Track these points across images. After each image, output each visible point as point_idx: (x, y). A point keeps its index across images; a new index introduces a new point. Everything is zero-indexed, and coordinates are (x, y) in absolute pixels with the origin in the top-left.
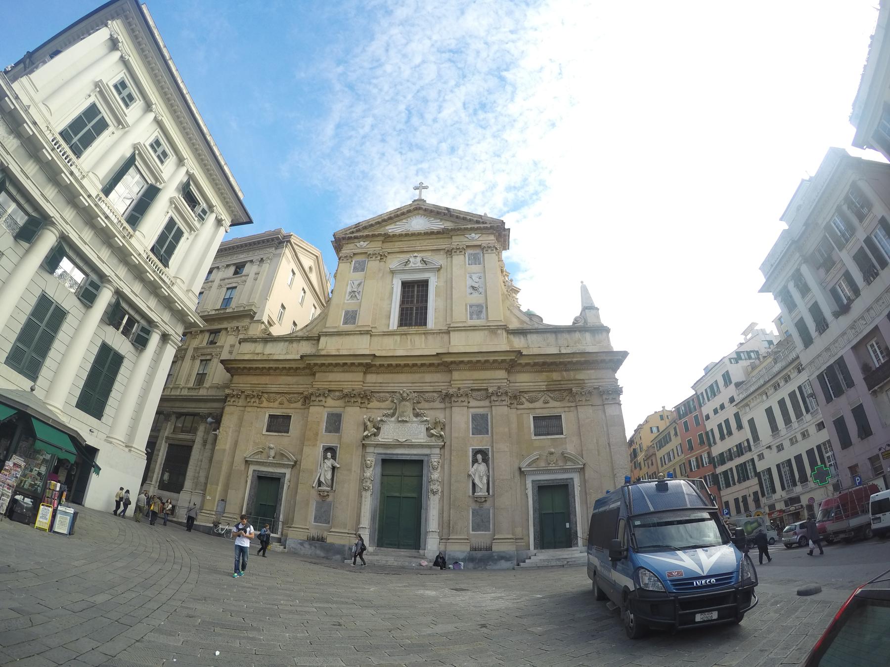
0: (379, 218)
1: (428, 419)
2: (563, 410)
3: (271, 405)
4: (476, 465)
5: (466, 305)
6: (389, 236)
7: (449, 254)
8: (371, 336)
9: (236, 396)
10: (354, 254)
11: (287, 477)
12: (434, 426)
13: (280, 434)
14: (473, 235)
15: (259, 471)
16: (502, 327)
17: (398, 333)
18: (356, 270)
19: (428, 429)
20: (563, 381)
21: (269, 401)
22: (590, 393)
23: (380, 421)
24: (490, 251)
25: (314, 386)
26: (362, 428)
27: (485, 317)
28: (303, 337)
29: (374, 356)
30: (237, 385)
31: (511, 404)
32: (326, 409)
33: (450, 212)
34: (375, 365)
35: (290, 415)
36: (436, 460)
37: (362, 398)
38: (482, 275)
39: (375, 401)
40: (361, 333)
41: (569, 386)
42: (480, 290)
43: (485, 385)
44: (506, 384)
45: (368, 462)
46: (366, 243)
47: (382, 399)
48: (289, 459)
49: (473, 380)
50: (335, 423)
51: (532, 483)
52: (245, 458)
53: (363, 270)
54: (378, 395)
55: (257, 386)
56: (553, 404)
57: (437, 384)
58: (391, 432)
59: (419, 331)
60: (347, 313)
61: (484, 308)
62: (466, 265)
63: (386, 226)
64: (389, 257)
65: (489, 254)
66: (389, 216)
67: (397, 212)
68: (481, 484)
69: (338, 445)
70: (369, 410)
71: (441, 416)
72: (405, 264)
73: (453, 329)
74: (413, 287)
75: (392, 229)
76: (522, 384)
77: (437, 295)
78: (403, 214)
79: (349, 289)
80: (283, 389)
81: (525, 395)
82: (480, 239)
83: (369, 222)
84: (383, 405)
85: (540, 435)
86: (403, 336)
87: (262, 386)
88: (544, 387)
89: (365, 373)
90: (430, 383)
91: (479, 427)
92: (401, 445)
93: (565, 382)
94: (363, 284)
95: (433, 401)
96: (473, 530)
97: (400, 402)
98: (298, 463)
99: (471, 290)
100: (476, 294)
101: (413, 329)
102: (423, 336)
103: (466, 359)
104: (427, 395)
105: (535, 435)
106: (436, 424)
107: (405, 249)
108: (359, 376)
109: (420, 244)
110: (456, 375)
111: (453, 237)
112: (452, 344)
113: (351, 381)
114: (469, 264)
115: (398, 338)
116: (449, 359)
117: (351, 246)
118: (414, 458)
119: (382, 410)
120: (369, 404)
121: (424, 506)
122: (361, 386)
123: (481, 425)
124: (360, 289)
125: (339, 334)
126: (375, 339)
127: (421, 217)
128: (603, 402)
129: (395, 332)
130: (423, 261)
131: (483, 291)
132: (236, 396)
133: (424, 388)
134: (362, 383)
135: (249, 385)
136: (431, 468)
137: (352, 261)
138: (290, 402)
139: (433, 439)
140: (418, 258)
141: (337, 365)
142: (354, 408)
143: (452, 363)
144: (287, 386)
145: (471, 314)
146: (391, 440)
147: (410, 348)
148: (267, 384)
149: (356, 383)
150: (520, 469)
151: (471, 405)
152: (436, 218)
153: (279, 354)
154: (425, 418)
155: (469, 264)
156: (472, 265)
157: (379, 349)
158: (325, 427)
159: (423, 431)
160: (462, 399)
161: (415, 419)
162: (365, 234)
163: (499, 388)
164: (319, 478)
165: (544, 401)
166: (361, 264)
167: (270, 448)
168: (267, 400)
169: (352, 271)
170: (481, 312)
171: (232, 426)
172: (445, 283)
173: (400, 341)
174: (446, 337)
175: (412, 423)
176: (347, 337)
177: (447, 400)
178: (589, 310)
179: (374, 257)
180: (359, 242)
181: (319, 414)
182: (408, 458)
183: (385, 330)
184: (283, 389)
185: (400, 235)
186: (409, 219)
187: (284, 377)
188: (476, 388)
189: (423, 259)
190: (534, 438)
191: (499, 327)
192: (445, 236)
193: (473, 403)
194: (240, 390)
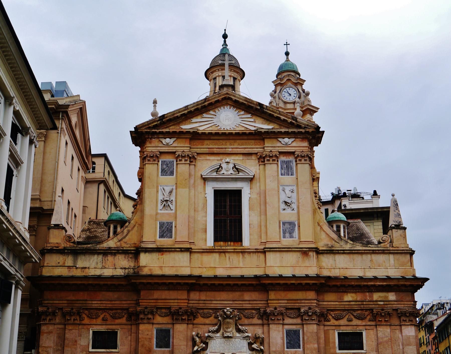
1: (250, 335)
2: (364, 328)
3: (94, 321)
5: (280, 223)
7: (262, 161)
8: (191, 252)
9: (51, 314)
10: (161, 153)
12: (254, 341)
13: (108, 350)
14: (286, 140)
16: (313, 250)
17: (217, 251)
18: (164, 172)
19: (250, 344)
20: (365, 302)
21: (90, 317)
22: (389, 314)
23: (207, 337)
24: (303, 161)
26: (190, 343)
28: (118, 250)
29: (200, 277)
30: (51, 302)
31: (319, 321)
32: (155, 326)
33: (264, 108)
34: (199, 284)
35: (116, 330)
37: (188, 316)
38: (295, 188)
39: (200, 317)
41: (371, 306)
42: (294, 206)
43: (297, 305)
44: (315, 304)
46: (172, 140)
47: (206, 315)
49: (287, 300)
53: (172, 173)
54: (201, 311)
55: (76, 302)
56: (356, 322)
57: (255, 302)
58: (217, 347)
59: (236, 249)
60: (162, 225)
62: (278, 175)
63: (193, 117)
64: (198, 158)
65: (303, 165)
66: (195, 108)
70: (195, 326)
71: (259, 331)
73: (268, 250)
76: (330, 303)
78: (211, 104)
79: (160, 197)
80: (105, 305)
81: (332, 313)
82: (294, 144)
83: (174, 114)
84: (207, 321)
86: (221, 254)
87: (81, 302)
88: (347, 306)
89: (189, 292)
90: (249, 301)
91: (292, 342)
93: (367, 303)
94: (174, 191)
95: (252, 318)
97: (225, 318)
99: (283, 206)
100: (289, 211)
101: (230, 246)
102: (241, 254)
103: (282, 282)
104: (246, 311)
105: (339, 350)
106: (256, 339)
107: (215, 151)
108: (183, 295)
109: (231, 145)
110: (272, 295)
111: (266, 140)
112: (268, 264)
114: (282, 175)
115: (216, 256)
117: (155, 142)
119: (206, 326)
120: (194, 320)
122: (186, 304)
124: (173, 198)
125: (160, 250)
126: (195, 256)
127: (230, 108)
128: (401, 323)
129: (212, 249)
130: (235, 168)
133: (244, 305)
134: (187, 301)
137: (158, 161)
138: (114, 318)
140: (230, 164)
142: (182, 325)
143: (269, 284)
144: (109, 302)
145: (284, 233)
147: (228, 266)
148: (86, 300)
149: (182, 301)
153: (95, 268)
154: (247, 334)
155: (282, 175)
156: (284, 175)
157: (200, 266)
158: (155, 343)
159: (245, 345)
161: (238, 335)
163: (310, 309)
165: (348, 319)
168: (88, 317)
170: (293, 230)
171: (52, 345)
172: (259, 195)
174: (262, 256)
175: (235, 339)
177: (264, 317)
178: (396, 230)
179: (183, 160)
180: (165, 138)
183: (204, 247)
184: (105, 305)
185: (210, 134)
187: (104, 293)
188: (290, 307)
189: (235, 166)
190: (338, 351)
191: (311, 249)
193: (288, 321)
194: (57, 308)
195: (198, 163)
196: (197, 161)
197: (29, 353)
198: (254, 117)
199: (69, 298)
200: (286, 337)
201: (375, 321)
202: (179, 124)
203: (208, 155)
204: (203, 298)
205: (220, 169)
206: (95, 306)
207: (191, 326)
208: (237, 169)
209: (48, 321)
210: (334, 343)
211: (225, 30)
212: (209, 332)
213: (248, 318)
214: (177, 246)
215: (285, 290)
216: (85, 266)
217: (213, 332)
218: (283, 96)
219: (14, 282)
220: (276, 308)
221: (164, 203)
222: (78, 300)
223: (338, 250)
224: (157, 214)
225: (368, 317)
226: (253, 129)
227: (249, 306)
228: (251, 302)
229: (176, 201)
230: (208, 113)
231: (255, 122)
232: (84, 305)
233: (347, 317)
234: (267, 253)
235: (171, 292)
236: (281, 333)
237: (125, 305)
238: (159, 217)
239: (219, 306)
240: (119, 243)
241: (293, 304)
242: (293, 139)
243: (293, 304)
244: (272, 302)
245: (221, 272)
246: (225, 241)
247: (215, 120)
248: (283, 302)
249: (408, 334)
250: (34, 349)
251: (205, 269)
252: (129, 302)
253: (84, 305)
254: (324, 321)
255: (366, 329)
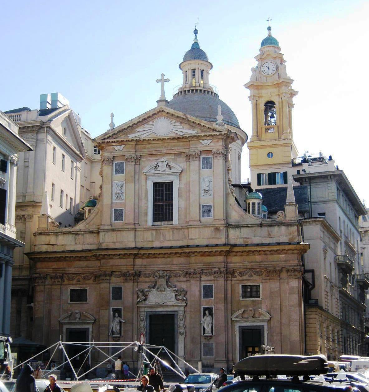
0: (130, 123)
3: (71, 282)
4: (205, 317)
5: (200, 205)
6: (140, 140)
8: (135, 230)
9: (42, 278)
11: (91, 330)
13: (81, 302)
14: (206, 141)
15: (70, 329)
17: (154, 229)
21: (69, 279)
24: (218, 157)
25: (101, 269)
26: (135, 296)
27: (213, 215)
28: (86, 231)
30: (42, 270)
31: (227, 278)
32: (111, 284)
34: (141, 254)
36: (182, 315)
40: (128, 230)
42: (211, 192)
43: (211, 266)
45: (142, 318)
48: (90, 319)
50: (118, 293)
51: (239, 328)
52: (59, 321)
53: (123, 172)
54: (144, 273)
55: (59, 269)
56: (255, 277)
57: (181, 265)
60: (116, 211)
61: (212, 207)
62: (199, 170)
63: (137, 127)
65: (218, 160)
67: (145, 116)
68: (208, 329)
69: (122, 308)
71: (184, 286)
72: (155, 167)
74: (162, 186)
75: (141, 133)
76: (235, 265)
77: (179, 196)
78: (149, 117)
81: (238, 271)
82: (212, 144)
84: (147, 280)
85: (246, 298)
87: (61, 269)
91: (207, 294)
92: (161, 306)
94: (124, 185)
96: (204, 356)
98: (97, 320)
99: (202, 193)
100: (207, 196)
107: (154, 152)
108: (130, 261)
110: (193, 259)
113: (125, 264)
116: (187, 250)
118: (169, 313)
120: (138, 279)
121: (176, 341)
123: (208, 292)
130: (168, 165)
131: (212, 193)
132: (42, 278)
135: (51, 270)
136: (179, 320)
139: (180, 301)
141: (114, 255)
143: (189, 252)
144: (81, 269)
145: (204, 212)
146: (154, 303)
148: (65, 268)
150: (232, 319)
151: (202, 279)
152: (177, 121)
153: (70, 245)
160: (195, 276)
161: (168, 289)
162: (120, 140)
163: (219, 269)
164: (112, 330)
166: (120, 166)
167: (77, 313)
169: (114, 173)
170: (210, 211)
173: (156, 235)
174: (186, 231)
176: (119, 232)
177: (188, 276)
180: (117, 146)
181: (106, 287)
182: (165, 313)
183: (145, 227)
186: (154, 121)
187: (77, 262)
189: (168, 164)
190: (241, 299)
192: (184, 140)
193: (204, 278)
195: (142, 164)
196: (141, 161)
197: (30, 305)
198: (182, 125)
199: (54, 267)
200: (203, 290)
201: (268, 276)
202: (127, 134)
203: (149, 157)
204: (145, 263)
205: (157, 166)
206: (70, 272)
207: (136, 284)
208: (169, 166)
209: (40, 283)
210: (239, 293)
211: (196, 26)
212: (149, 288)
213: (175, 276)
214: (126, 227)
215: (201, 256)
216: (63, 244)
217: (150, 288)
218: (263, 70)
219: (4, 262)
220: (195, 270)
221: (117, 195)
222: (59, 268)
223: (243, 225)
224: (112, 203)
225: (265, 274)
226: (181, 134)
227: (176, 268)
228: (179, 266)
229: (125, 193)
230: (148, 123)
231: (183, 128)
232: (64, 271)
233: (249, 274)
234: (189, 229)
235: (122, 260)
236: (199, 287)
237: (92, 271)
238: (114, 205)
239: (156, 269)
240: (87, 226)
241: (207, 266)
242: (211, 140)
243: (207, 266)
244: (192, 265)
245: (157, 244)
246: (161, 221)
247: (153, 129)
248: (201, 264)
249: (293, 286)
250: (32, 302)
251: (145, 243)
252: (94, 268)
253: (64, 271)
254: (232, 277)
255: (262, 283)
